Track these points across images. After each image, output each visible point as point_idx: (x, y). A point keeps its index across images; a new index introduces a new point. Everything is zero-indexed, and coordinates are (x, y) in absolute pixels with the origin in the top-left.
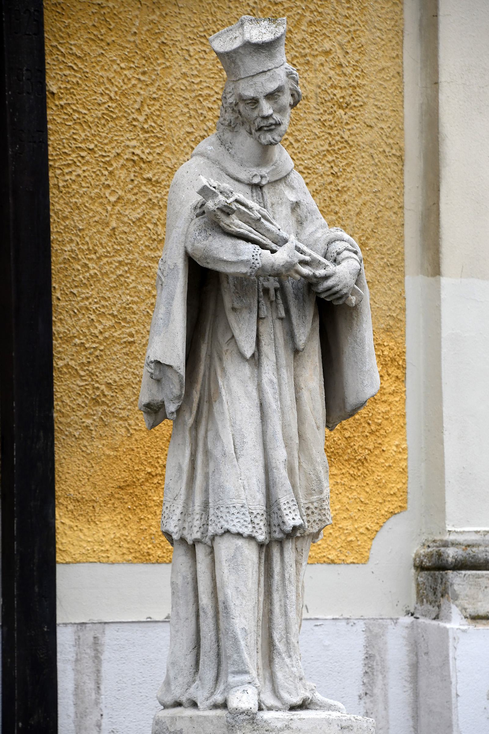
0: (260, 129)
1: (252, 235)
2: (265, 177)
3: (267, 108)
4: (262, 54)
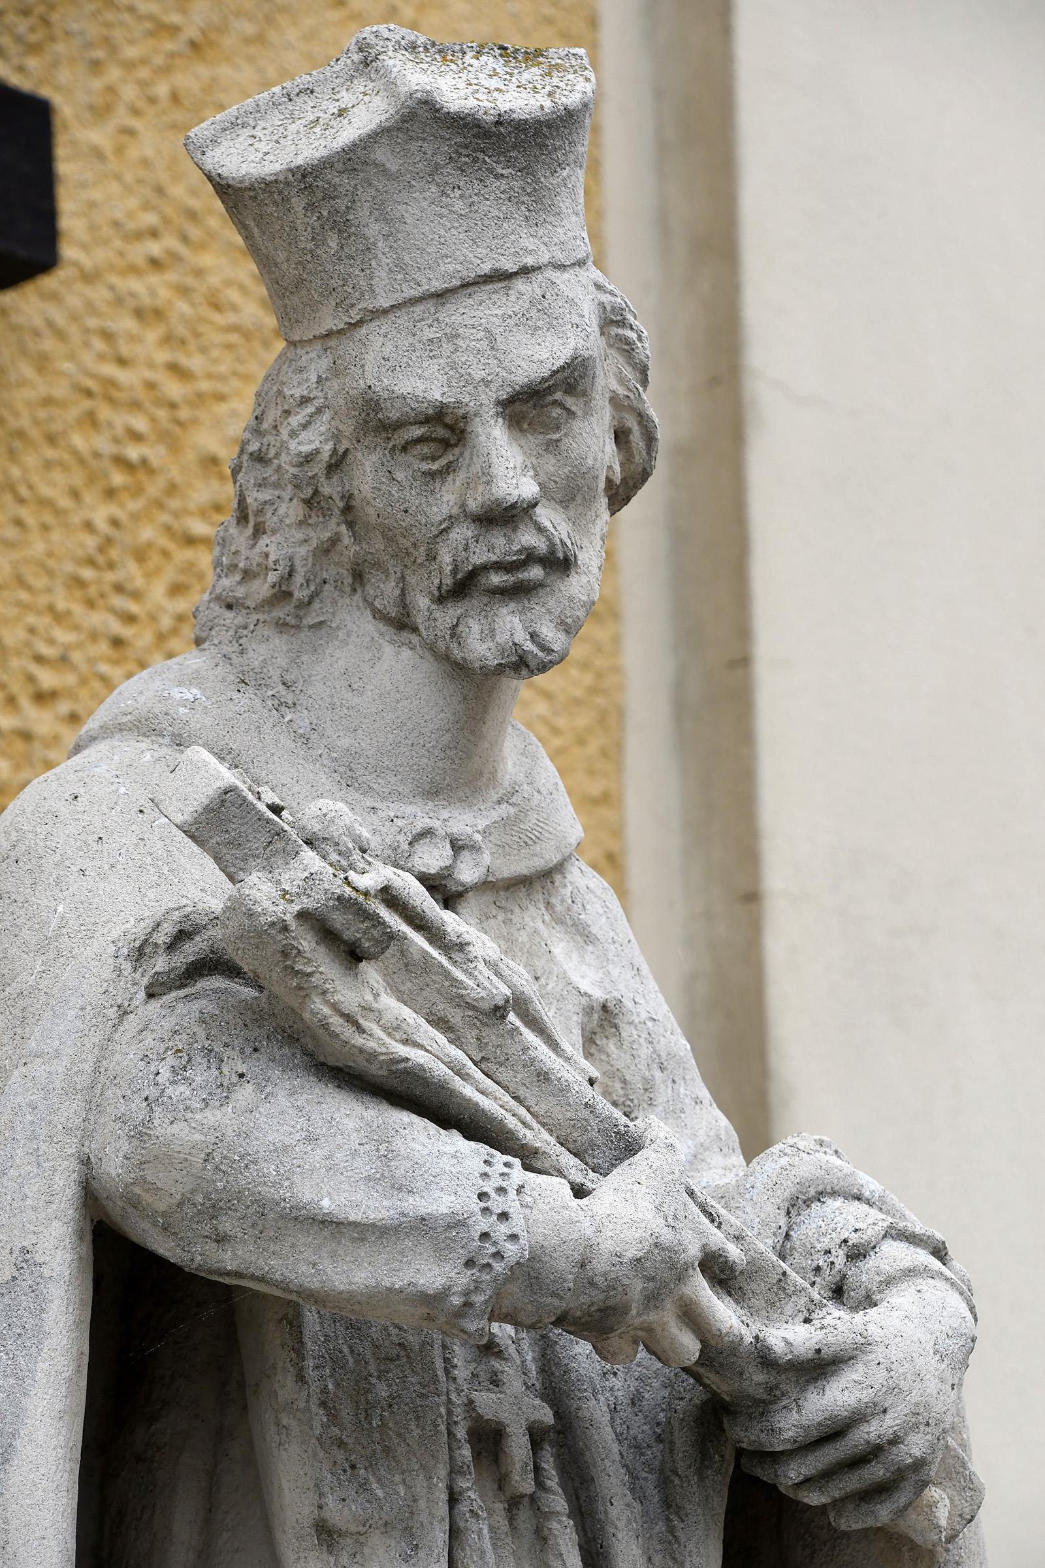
1: (468, 1091)
2: (474, 848)
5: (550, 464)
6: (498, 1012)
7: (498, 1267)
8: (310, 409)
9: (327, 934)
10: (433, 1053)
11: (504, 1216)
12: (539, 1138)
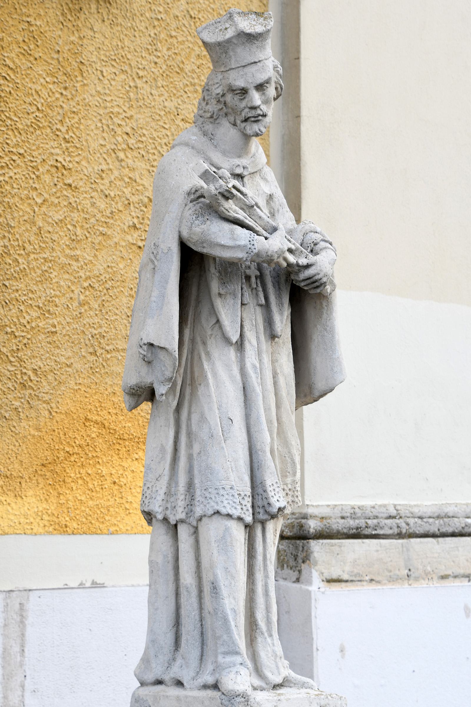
0: (246, 120)
1: (247, 221)
2: (247, 168)
3: (256, 98)
4: (254, 45)
5: (263, 97)
6: (253, 206)
7: (252, 254)
8: (218, 85)
9: (223, 196)
10: (241, 215)
11: (253, 245)
12: (259, 229)
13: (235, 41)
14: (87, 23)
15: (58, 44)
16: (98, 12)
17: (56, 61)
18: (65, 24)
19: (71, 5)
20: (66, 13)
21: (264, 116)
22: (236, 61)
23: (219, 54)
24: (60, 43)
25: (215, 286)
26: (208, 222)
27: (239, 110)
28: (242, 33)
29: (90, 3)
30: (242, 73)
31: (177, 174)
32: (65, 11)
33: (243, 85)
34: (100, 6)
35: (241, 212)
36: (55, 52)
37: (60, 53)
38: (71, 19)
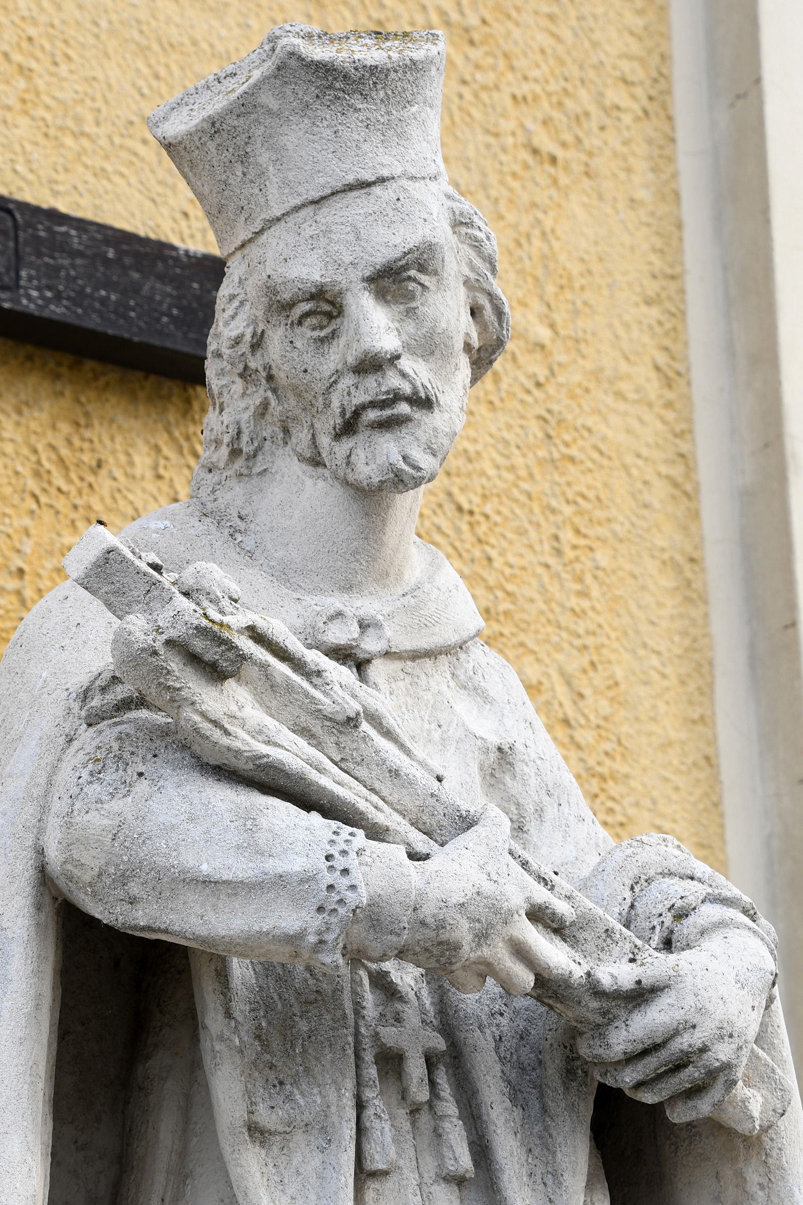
0: (349, 426)
1: (324, 781)
2: (378, 625)
3: (376, 325)
4: (353, 117)
5: (410, 327)
6: (352, 722)
7: (342, 911)
8: (236, 303)
9: (194, 659)
10: (293, 753)
11: (345, 872)
12: (385, 817)
13: (268, 99)
14: (122, 503)
15: (18, 551)
16: (159, 477)
17: (14, 599)
18: (43, 499)
19: (64, 452)
20: (49, 472)
21: (425, 403)
22: (286, 183)
23: (219, 170)
24: (28, 548)
25: (229, 1089)
26: (142, 787)
27: (320, 387)
28: (293, 62)
29: (131, 451)
30: (309, 231)
31: (66, 642)
32: (47, 465)
33: (317, 277)
34: (162, 462)
35: (286, 736)
36: (10, 573)
37: (27, 577)
38: (65, 488)
